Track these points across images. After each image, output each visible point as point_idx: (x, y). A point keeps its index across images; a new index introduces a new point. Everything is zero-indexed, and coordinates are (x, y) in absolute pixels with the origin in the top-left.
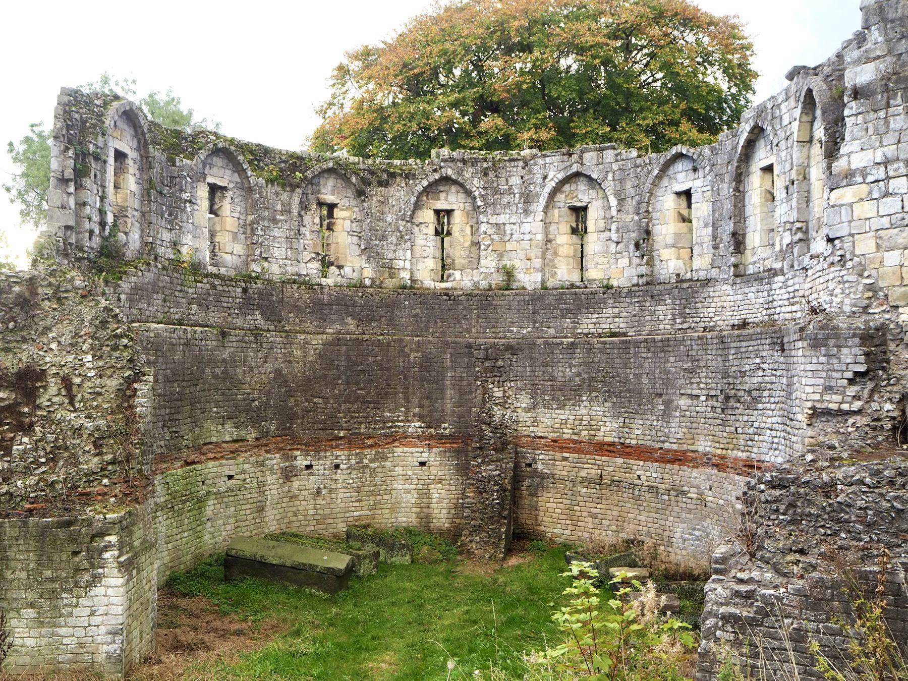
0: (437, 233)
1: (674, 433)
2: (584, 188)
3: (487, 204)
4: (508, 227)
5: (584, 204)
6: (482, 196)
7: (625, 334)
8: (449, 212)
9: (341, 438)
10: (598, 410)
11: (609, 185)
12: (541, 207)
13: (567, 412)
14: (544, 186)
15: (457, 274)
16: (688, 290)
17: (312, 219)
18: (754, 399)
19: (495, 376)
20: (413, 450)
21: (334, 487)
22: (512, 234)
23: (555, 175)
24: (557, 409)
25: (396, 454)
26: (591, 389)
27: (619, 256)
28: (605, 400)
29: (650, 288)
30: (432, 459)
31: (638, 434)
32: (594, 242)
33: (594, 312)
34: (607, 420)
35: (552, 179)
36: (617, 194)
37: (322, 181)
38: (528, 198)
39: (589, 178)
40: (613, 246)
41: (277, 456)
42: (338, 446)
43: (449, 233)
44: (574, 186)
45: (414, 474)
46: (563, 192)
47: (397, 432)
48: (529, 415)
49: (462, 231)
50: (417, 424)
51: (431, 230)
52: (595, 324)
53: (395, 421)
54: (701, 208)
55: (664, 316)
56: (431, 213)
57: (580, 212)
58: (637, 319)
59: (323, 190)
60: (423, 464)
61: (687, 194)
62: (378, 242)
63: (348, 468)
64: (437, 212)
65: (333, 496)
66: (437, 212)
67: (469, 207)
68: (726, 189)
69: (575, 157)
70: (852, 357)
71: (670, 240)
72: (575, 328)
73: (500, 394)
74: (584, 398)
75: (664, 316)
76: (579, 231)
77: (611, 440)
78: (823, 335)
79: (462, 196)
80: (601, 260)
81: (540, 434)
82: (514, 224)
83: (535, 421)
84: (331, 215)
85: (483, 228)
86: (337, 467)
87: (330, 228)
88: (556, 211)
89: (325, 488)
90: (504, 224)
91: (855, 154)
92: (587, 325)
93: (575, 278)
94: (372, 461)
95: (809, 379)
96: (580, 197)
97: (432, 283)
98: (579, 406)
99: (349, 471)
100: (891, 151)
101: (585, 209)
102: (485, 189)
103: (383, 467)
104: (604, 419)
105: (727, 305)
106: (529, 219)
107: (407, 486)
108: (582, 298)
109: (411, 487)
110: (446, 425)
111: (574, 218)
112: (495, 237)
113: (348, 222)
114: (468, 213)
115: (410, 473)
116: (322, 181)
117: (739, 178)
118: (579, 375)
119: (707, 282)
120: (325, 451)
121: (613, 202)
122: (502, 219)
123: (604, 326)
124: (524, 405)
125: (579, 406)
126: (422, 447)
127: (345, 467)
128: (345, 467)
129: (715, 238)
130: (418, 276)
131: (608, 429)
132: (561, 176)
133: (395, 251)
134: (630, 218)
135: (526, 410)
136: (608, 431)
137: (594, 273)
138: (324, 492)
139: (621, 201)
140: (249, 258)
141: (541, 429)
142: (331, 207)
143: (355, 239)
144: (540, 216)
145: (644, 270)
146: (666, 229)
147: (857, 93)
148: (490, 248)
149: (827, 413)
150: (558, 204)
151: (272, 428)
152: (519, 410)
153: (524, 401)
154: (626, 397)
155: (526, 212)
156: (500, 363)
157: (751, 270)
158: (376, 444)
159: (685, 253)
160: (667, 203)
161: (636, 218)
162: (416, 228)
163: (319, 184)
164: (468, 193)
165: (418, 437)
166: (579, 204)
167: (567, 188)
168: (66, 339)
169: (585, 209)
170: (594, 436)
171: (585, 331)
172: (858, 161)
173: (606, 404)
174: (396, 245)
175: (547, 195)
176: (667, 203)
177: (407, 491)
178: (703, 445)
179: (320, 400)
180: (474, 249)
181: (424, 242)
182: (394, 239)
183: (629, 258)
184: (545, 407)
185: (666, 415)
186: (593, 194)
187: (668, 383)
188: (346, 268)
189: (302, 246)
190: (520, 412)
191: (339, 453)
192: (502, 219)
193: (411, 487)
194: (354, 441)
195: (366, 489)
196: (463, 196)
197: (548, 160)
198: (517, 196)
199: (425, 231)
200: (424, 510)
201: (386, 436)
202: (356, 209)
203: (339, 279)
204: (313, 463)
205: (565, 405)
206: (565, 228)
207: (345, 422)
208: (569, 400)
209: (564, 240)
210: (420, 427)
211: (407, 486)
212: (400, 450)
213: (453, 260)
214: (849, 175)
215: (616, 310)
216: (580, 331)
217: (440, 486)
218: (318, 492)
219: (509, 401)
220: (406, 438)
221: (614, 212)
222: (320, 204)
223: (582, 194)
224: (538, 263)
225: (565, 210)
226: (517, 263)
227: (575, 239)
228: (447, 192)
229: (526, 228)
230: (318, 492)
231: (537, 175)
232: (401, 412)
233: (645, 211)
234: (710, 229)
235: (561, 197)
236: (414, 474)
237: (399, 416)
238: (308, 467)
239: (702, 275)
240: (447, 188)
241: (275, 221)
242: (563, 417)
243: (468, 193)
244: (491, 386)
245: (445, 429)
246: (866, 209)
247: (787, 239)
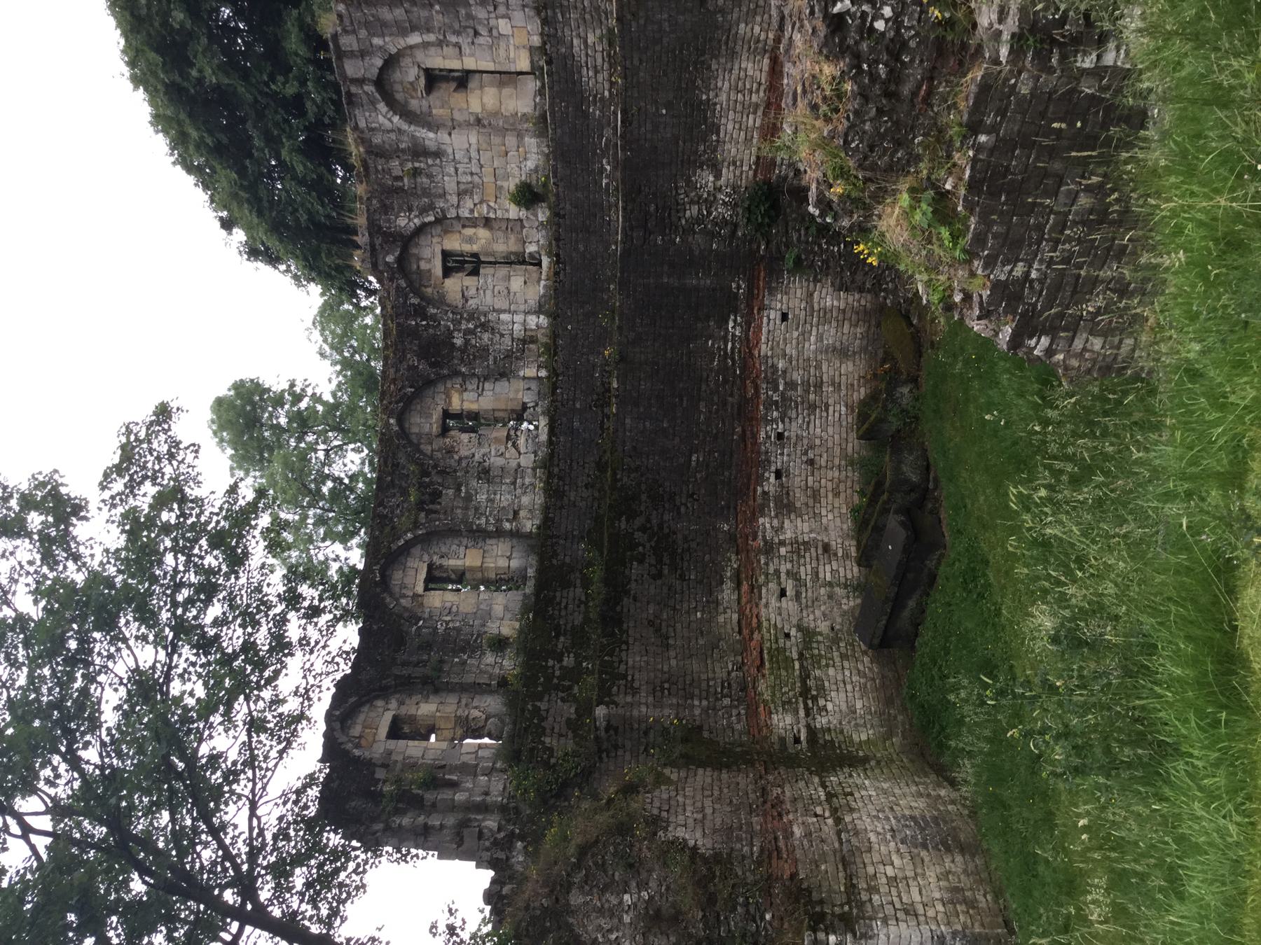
0: (475, 272)
2: (398, 74)
3: (431, 207)
4: (464, 179)
5: (422, 73)
6: (421, 214)
7: (610, 31)
8: (446, 255)
9: (744, 431)
11: (393, 44)
12: (431, 135)
13: (723, 121)
14: (399, 130)
15: (532, 248)
17: (464, 443)
19: (670, 215)
20: (764, 330)
21: (805, 441)
22: (472, 174)
23: (384, 118)
24: (718, 135)
25: (769, 353)
27: (495, 33)
28: (709, 68)
30: (779, 306)
33: (580, 72)
34: (736, 67)
35: (389, 119)
36: (404, 32)
37: (415, 430)
38: (419, 151)
40: (480, 40)
41: (761, 520)
42: (755, 436)
43: (475, 255)
44: (398, 87)
45: (797, 329)
46: (406, 102)
47: (740, 352)
48: (724, 171)
49: (470, 240)
50: (731, 324)
51: (470, 281)
52: (596, 72)
53: (726, 353)
56: (449, 282)
57: (433, 79)
59: (426, 429)
60: (784, 317)
62: (491, 358)
63: (783, 422)
64: (447, 272)
65: (818, 442)
66: (447, 272)
67: (438, 230)
69: (354, 89)
72: (603, 98)
73: (695, 209)
74: (704, 97)
76: (463, 80)
77: (766, 61)
79: (423, 240)
80: (502, 52)
81: (753, 158)
82: (456, 169)
83: (734, 163)
84: (458, 416)
85: (465, 213)
86: (780, 436)
87: (475, 416)
88: (434, 111)
89: (806, 453)
90: (458, 183)
92: (598, 79)
93: (532, 85)
94: (776, 389)
96: (412, 79)
97: (543, 283)
98: (715, 104)
99: (787, 420)
102: (410, 210)
103: (784, 372)
104: (735, 72)
106: (450, 151)
107: (813, 339)
109: (814, 333)
110: (734, 285)
111: (444, 85)
112: (477, 199)
113: (465, 395)
114: (446, 232)
115: (795, 334)
116: (415, 430)
118: (668, 106)
120: (759, 453)
121: (415, 39)
123: (599, 61)
124: (711, 179)
125: (715, 104)
126: (762, 318)
127: (781, 426)
128: (781, 426)
130: (533, 300)
131: (750, 65)
132: (382, 107)
133: (502, 335)
135: (718, 176)
137: (524, 64)
138: (811, 455)
139: (414, 28)
140: (516, 535)
141: (746, 158)
142: (447, 414)
143: (487, 385)
144: (443, 136)
148: (492, 204)
150: (425, 109)
151: (726, 528)
152: (719, 183)
153: (706, 179)
156: (653, 207)
158: (753, 382)
161: (437, 7)
162: (470, 302)
163: (419, 435)
165: (748, 324)
166: (422, 81)
167: (399, 96)
168: (605, 923)
170: (760, 84)
171: (607, 86)
173: (714, 67)
174: (493, 334)
175: (412, 128)
177: (820, 338)
179: (694, 458)
180: (496, 226)
181: (489, 293)
182: (486, 336)
183: (497, 18)
184: (715, 150)
186: (406, 61)
188: (526, 400)
189: (498, 459)
190: (723, 181)
191: (763, 434)
192: (450, 185)
193: (814, 333)
194: (747, 414)
195: (812, 397)
196: (422, 238)
197: (362, 124)
198: (417, 165)
199: (472, 292)
200: (848, 315)
201: (743, 369)
202: (449, 385)
203: (539, 409)
204: (773, 468)
205: (713, 124)
206: (457, 99)
207: (724, 423)
208: (705, 118)
210: (735, 321)
211: (813, 339)
212: (763, 347)
213: (511, 253)
215: (576, 42)
216: (607, 93)
217: (816, 295)
218: (811, 462)
219: (705, 195)
220: (748, 340)
221: (431, 37)
222: (445, 430)
223: (410, 73)
225: (431, 97)
227: (473, 84)
228: (419, 259)
230: (811, 462)
231: (385, 138)
232: (713, 344)
235: (414, 104)
236: (797, 329)
237: (719, 348)
238: (778, 474)
240: (413, 260)
241: (469, 498)
242: (730, 127)
243: (421, 230)
244: (683, 222)
245: (739, 287)
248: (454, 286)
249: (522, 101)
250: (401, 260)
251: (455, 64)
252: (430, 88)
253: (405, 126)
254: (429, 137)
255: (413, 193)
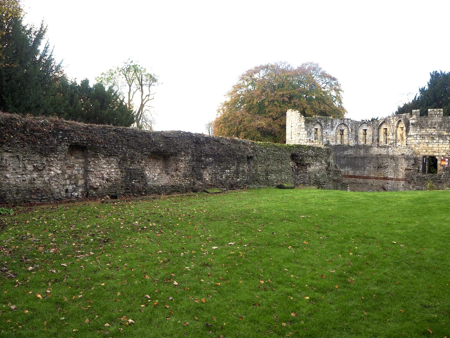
1: (366, 173)
8: (316, 129)
10: (349, 169)
16: (367, 148)
18: (385, 167)
23: (338, 123)
26: (348, 165)
29: (357, 147)
31: (358, 173)
32: (345, 137)
38: (332, 127)
39: (345, 125)
54: (369, 133)
55: (362, 152)
57: (342, 131)
58: (355, 152)
61: (365, 130)
68: (376, 131)
70: (412, 162)
71: (362, 138)
75: (362, 152)
76: (342, 134)
78: (407, 158)
91: (411, 133)
95: (403, 165)
100: (417, 133)
101: (343, 130)
105: (375, 151)
108: (342, 148)
117: (379, 129)
119: (371, 147)
121: (350, 130)
122: (327, 131)
129: (373, 139)
134: (353, 133)
136: (351, 173)
137: (345, 143)
139: (352, 130)
144: (335, 131)
145: (356, 143)
146: (361, 136)
147: (412, 124)
149: (408, 169)
154: (355, 167)
155: (332, 130)
157: (380, 145)
159: (364, 140)
160: (361, 131)
164: (321, 125)
169: (343, 130)
172: (412, 134)
176: (361, 131)
178: (372, 175)
185: (364, 170)
187: (365, 164)
206: (339, 134)
209: (339, 136)
214: (411, 136)
223: (343, 127)
224: (334, 140)
226: (330, 140)
229: (332, 133)
233: (356, 132)
234: (371, 137)
239: (369, 145)
243: (321, 125)
246: (414, 141)
247: (392, 142)
248: (313, 129)
249: (339, 143)
250: (318, 122)
251: (344, 134)
252: (341, 130)
253: (337, 126)
254: (335, 129)
255: (326, 125)
